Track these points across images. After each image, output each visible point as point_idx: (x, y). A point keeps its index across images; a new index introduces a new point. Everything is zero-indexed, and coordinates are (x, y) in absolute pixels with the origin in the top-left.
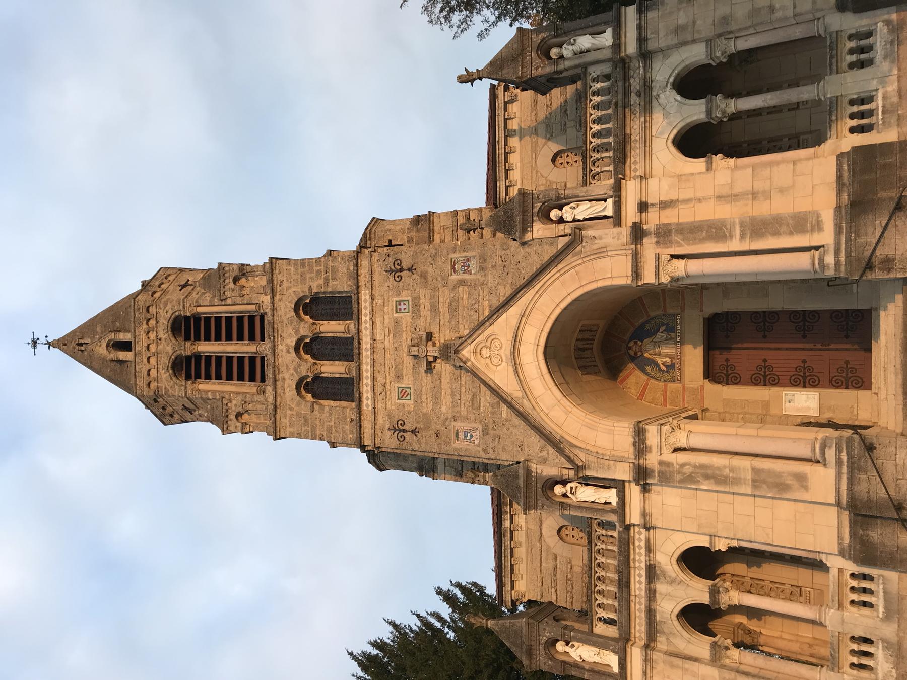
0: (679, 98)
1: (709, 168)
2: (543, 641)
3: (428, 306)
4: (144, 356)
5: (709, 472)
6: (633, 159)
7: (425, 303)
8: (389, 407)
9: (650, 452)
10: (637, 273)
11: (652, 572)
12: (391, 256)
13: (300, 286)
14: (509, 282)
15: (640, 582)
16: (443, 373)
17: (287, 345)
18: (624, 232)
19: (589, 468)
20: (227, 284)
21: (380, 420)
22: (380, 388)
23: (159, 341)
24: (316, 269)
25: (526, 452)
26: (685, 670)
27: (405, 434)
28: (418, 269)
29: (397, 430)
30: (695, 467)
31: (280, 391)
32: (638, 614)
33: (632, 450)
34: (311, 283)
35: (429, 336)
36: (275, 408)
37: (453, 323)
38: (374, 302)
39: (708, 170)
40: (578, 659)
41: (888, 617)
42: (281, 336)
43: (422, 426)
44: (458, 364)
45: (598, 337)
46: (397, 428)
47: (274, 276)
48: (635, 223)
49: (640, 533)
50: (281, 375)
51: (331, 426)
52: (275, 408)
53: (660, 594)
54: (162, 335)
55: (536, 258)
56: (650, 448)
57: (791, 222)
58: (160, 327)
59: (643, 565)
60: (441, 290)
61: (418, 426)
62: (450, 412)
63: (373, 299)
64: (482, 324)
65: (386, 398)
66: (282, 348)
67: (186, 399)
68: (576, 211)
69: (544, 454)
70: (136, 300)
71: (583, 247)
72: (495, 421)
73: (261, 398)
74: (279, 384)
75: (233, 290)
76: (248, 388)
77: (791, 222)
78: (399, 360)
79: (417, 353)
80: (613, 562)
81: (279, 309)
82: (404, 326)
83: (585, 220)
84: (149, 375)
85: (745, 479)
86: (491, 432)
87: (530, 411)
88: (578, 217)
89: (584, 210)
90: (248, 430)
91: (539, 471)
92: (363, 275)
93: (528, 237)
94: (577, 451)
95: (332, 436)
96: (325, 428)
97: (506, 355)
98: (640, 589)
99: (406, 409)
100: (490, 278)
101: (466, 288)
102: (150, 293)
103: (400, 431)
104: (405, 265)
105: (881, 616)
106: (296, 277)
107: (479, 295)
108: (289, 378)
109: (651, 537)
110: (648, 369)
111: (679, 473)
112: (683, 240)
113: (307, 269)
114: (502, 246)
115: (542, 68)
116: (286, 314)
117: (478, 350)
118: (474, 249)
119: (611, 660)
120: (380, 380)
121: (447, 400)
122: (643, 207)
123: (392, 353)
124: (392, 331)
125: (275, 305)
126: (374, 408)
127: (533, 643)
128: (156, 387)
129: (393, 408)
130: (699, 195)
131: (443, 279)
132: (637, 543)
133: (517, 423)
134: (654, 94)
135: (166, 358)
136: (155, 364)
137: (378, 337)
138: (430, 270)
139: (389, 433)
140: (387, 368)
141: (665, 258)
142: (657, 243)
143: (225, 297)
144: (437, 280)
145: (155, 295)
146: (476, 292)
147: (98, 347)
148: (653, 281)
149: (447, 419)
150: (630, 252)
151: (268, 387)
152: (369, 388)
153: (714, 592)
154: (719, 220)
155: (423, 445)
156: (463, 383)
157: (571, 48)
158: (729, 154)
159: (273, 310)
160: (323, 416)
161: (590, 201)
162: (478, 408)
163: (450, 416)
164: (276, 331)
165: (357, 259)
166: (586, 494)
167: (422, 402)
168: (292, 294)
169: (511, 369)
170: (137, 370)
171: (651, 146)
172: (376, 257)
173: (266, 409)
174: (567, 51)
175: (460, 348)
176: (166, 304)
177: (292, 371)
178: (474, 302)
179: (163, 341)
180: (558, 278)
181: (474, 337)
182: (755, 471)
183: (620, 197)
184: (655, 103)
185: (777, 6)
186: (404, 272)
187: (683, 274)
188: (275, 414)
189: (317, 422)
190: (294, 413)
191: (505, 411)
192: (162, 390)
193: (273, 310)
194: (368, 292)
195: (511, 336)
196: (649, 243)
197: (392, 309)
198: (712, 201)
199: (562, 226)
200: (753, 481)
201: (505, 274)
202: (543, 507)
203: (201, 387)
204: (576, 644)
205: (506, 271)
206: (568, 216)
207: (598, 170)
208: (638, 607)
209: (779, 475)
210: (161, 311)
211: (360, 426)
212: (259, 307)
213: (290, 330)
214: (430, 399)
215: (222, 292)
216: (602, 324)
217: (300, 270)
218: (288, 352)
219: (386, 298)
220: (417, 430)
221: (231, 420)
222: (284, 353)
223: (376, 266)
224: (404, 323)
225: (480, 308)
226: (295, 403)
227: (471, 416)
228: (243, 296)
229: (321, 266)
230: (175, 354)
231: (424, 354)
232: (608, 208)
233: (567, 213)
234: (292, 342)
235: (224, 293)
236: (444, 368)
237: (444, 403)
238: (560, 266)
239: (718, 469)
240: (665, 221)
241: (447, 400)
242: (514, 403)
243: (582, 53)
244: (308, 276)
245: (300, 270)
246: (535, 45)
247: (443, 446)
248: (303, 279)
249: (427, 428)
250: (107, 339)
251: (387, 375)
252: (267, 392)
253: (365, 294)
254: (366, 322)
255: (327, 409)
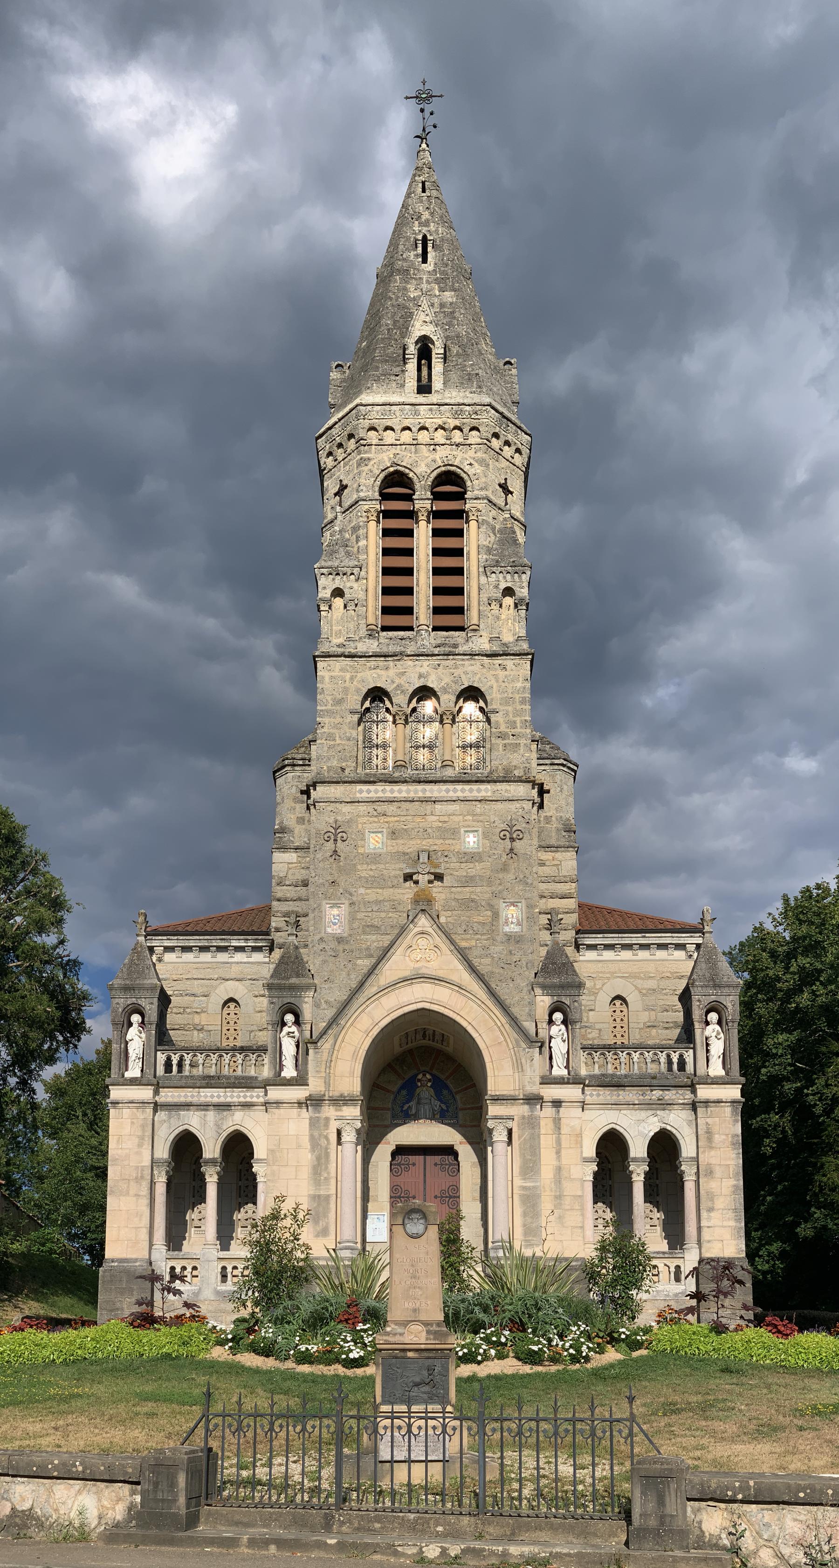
0: (652, 1134)
1: (586, 1160)
2: (140, 1002)
3: (472, 872)
4: (412, 421)
5: (323, 1161)
6: (601, 1093)
7: (476, 869)
8: (361, 820)
9: (336, 1110)
10: (497, 1099)
11: (224, 1107)
12: (527, 826)
13: (499, 696)
14: (494, 970)
15: (212, 1096)
16: (400, 891)
17: (428, 674)
18: (534, 1088)
19: (316, 1053)
20: (505, 578)
21: (346, 808)
22: (381, 808)
23: (432, 447)
24: (518, 719)
25: (323, 986)
26: (142, 1138)
27: (332, 841)
28: (511, 861)
29: (336, 829)
30: (327, 1149)
31: (373, 662)
32: (183, 1094)
33: (336, 1094)
34: (501, 713)
35: (439, 877)
36: (352, 656)
37: (453, 904)
38: (477, 803)
39: (584, 1158)
40: (128, 1037)
41: (218, 1293)
42: (439, 665)
43: (341, 864)
44: (410, 913)
45: (438, 1046)
46: (339, 831)
47: (512, 657)
48: (542, 1098)
49: (258, 1097)
50: (391, 663)
51: (334, 740)
52: (352, 656)
53: (205, 1115)
54: (442, 453)
55: (517, 998)
56: (340, 1110)
57: (534, 1225)
58: (451, 450)
59: (229, 1100)
60: (488, 889)
61: (342, 859)
62: (360, 898)
63: (480, 801)
64: (452, 942)
65: (371, 817)
66: (425, 665)
67: (355, 497)
68: (559, 1040)
69: (324, 1005)
70: (488, 407)
71: (524, 1049)
72: (352, 951)
73: (363, 632)
74: (381, 662)
75: (497, 587)
76: (374, 602)
77: (534, 1225)
78: (414, 833)
79: (421, 860)
80: (226, 1071)
81: (472, 662)
82: (450, 842)
83: (550, 1048)
84: (388, 428)
85: (320, 1189)
86: (341, 948)
87: (366, 993)
88: (553, 1040)
89: (559, 1047)
90: (322, 608)
91: (306, 999)
92: (508, 788)
93: (538, 991)
94: (331, 1041)
95: (323, 741)
96: (332, 731)
97: (419, 968)
98: (206, 1096)
99: (360, 843)
100: (499, 948)
101: (490, 919)
102: (497, 430)
103: (336, 835)
104: (517, 844)
105: (219, 1288)
106: (510, 691)
107: (482, 935)
108: (388, 677)
109: (256, 1108)
110: (404, 1092)
111: (320, 1135)
112: (525, 1139)
113: (519, 707)
114: (531, 962)
115: (699, 1006)
116: (466, 673)
117: (425, 936)
118: (529, 929)
119: (134, 1072)
120: (391, 808)
121: (372, 895)
122: (557, 1104)
123: (421, 825)
124: (445, 825)
125: (476, 657)
126: (359, 802)
127: (137, 992)
128: (369, 441)
129: (360, 826)
130: (563, 1152)
131: (500, 892)
132: (248, 1094)
133: (353, 976)
134: (658, 1112)
135: (410, 461)
136: (401, 442)
137: (438, 806)
138: (510, 876)
139: (331, 820)
140: (403, 819)
141: (510, 1124)
142: (523, 1117)
143: (488, 574)
144: (500, 884)
145: (494, 439)
146: (485, 931)
147: (422, 317)
148: (490, 1113)
149: (351, 894)
150: (517, 1093)
151: (376, 643)
152: (380, 794)
153: (213, 1162)
154: (539, 1169)
155: (321, 865)
156: (390, 915)
157: (714, 1034)
158: (596, 1175)
159: (470, 655)
160: (345, 728)
161: (568, 1052)
162: (364, 933)
163: (354, 899)
164: (445, 657)
165: (527, 781)
166: (289, 1048)
167: (368, 864)
168: (489, 684)
169: (407, 973)
170: (394, 408)
171: (611, 1109)
172: (528, 805)
173: (349, 639)
174: (713, 1030)
175: (427, 916)
176: (481, 462)
177: (397, 681)
178: (475, 929)
179: (432, 456)
180: (496, 1024)
181: (440, 932)
182: (328, 1197)
183: (568, 1083)
184: (651, 1112)
185: (712, 1214)
186: (509, 843)
187: (495, 1139)
188: (346, 656)
189: (338, 720)
190: (347, 684)
191: (365, 964)
192: (366, 452)
193: (470, 655)
194: (489, 794)
195: (441, 974)
196: (524, 1110)
197: (469, 826)
198: (555, 1163)
199: (545, 1025)
200: (319, 1196)
201: (502, 965)
202: (272, 1003)
203: (372, 525)
204: (143, 1035)
205: (506, 966)
206: (554, 1030)
207: (596, 1059)
208: (189, 1094)
209: (325, 1215)
210: (471, 453)
211: (337, 782)
212: (475, 630)
213: (447, 680)
214: (371, 873)
215: (494, 569)
216: (450, 1049)
217: (517, 696)
218: (420, 676)
219: (481, 818)
220: (337, 857)
221: (334, 579)
222: (418, 669)
223: (518, 805)
224: (454, 842)
225: (468, 936)
226: (360, 686)
227: (356, 925)
228: (490, 604)
229: (521, 727)
230: (415, 477)
231: (420, 870)
232: (559, 1071)
233: (558, 1030)
234: (432, 682)
235: (494, 572)
236: (408, 891)
237: (369, 891)
238: (507, 1026)
239: (327, 1168)
240: (542, 1123)
241: (372, 895)
242: (373, 977)
243: (708, 1045)
244: (510, 709)
245: (517, 696)
246: (722, 999)
247: (323, 889)
248: (507, 701)
249: (340, 870)
250: (434, 338)
251: (396, 819)
252: (371, 641)
253: (486, 790)
254: (455, 791)
255: (354, 733)
